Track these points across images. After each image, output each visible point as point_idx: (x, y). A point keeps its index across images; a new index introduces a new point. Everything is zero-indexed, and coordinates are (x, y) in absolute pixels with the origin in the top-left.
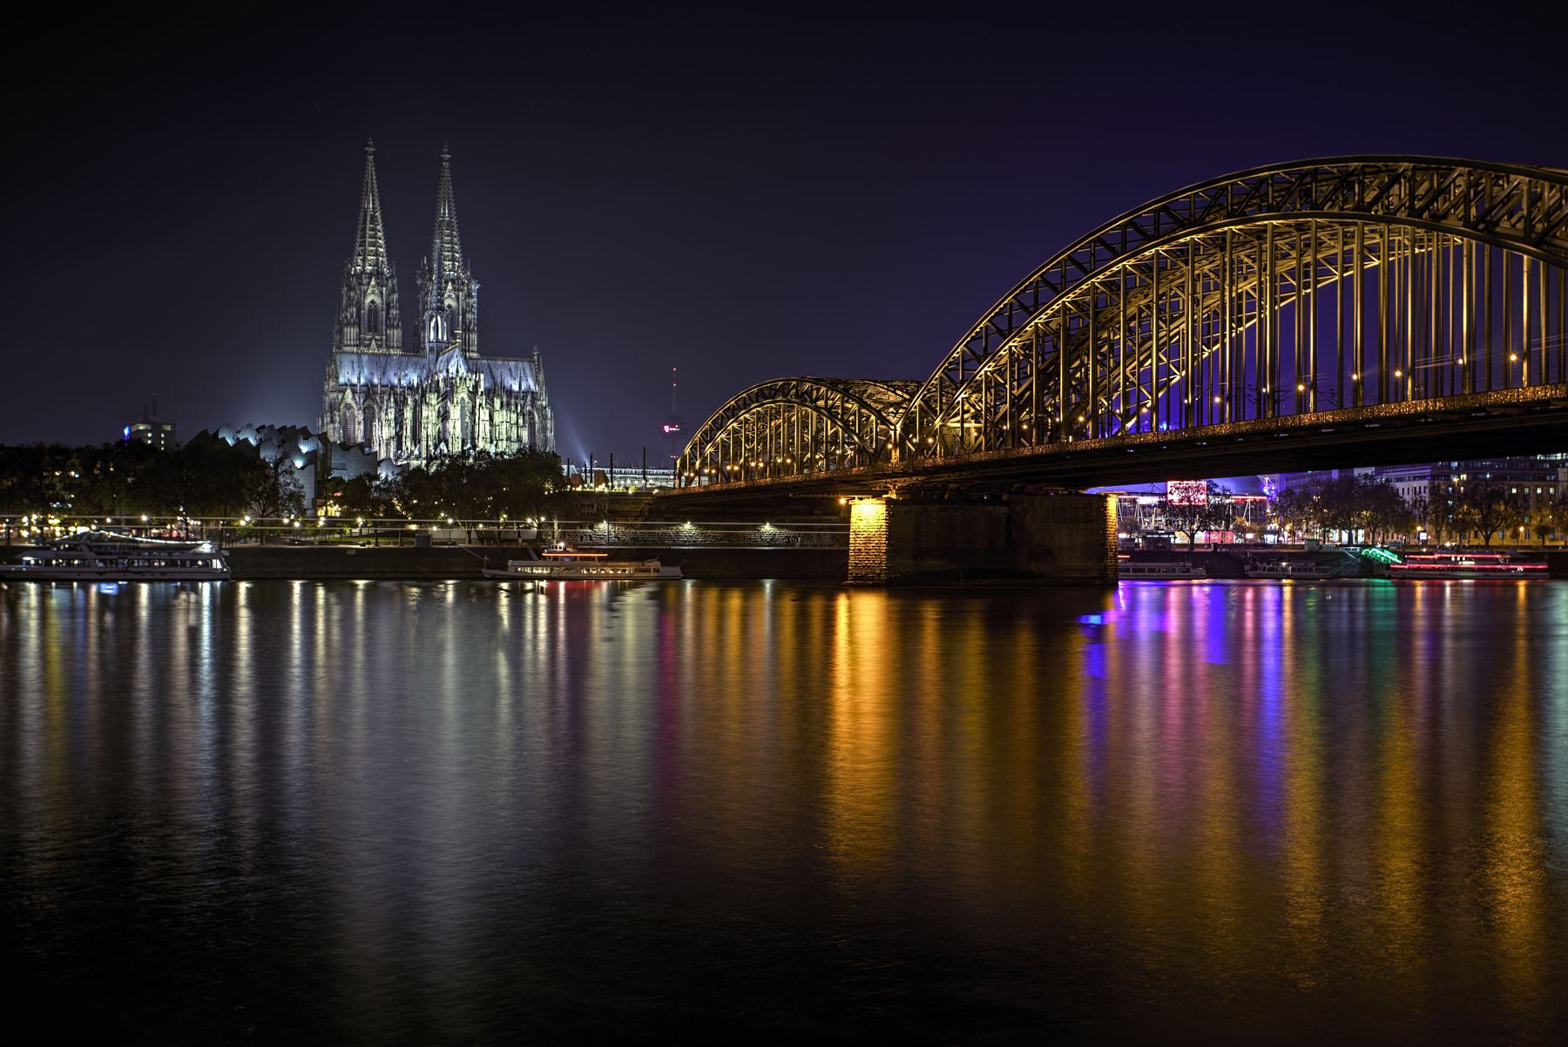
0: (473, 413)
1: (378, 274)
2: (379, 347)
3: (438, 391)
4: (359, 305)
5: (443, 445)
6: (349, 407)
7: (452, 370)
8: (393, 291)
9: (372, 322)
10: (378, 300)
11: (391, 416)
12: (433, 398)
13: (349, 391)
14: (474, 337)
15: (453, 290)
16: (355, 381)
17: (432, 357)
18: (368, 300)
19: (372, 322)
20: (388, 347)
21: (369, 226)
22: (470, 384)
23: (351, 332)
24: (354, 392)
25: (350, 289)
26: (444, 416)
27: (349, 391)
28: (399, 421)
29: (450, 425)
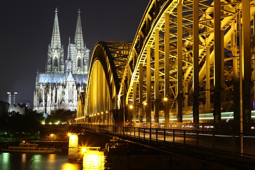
0: (73, 92)
1: (57, 48)
2: (58, 70)
4: (51, 59)
5: (63, 102)
6: (41, 90)
7: (68, 79)
10: (57, 57)
11: (50, 93)
12: (61, 87)
13: (41, 85)
16: (43, 82)
20: (60, 70)
21: (55, 34)
23: (49, 66)
24: (43, 85)
25: (49, 53)
26: (64, 93)
27: (41, 85)
28: (52, 95)
29: (65, 95)
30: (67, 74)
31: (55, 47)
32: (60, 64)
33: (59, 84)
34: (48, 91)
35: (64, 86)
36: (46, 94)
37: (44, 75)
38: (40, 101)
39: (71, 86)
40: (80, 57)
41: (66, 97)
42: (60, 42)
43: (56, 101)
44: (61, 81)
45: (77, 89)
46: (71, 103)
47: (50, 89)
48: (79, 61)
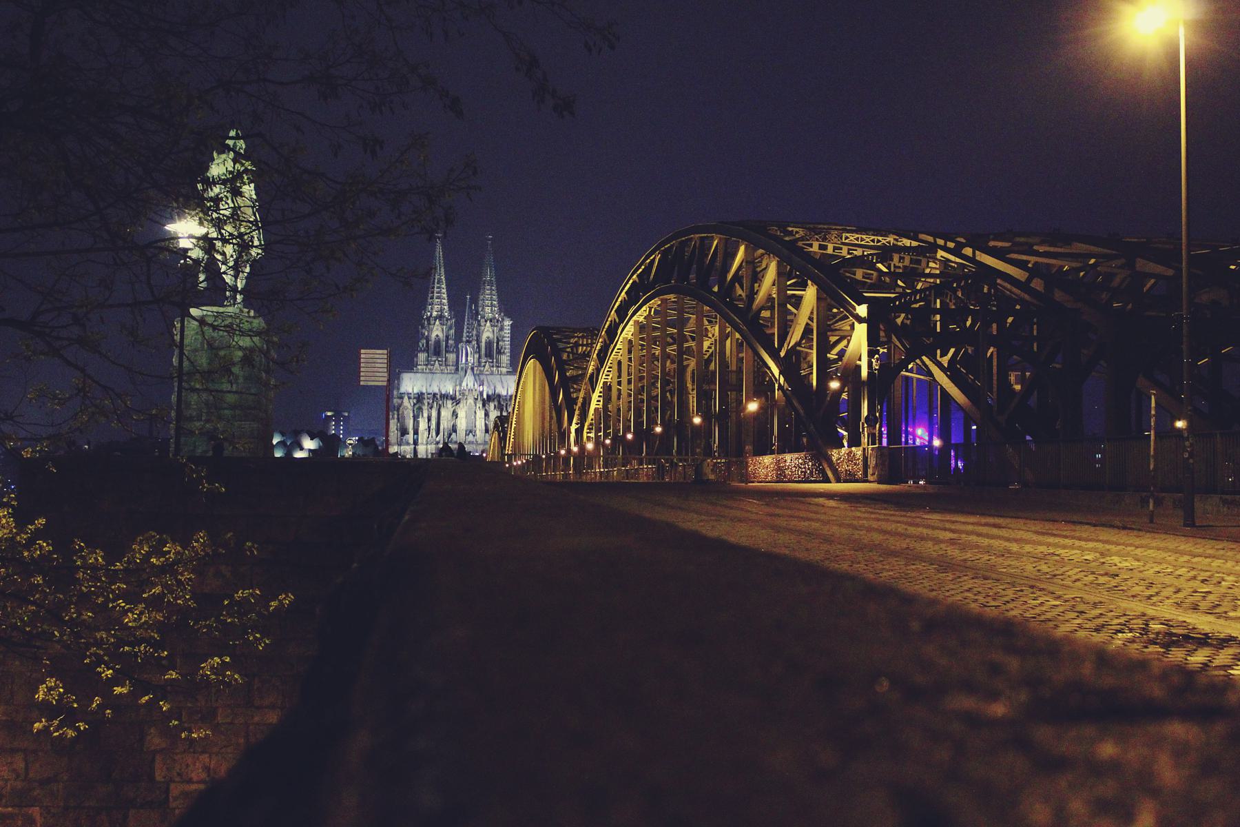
1: (440, 317)
3: (453, 398)
4: (428, 339)
7: (464, 384)
8: (450, 328)
9: (437, 350)
10: (441, 335)
11: (426, 415)
12: (449, 402)
14: (505, 359)
15: (493, 325)
17: (462, 373)
18: (434, 335)
19: (437, 350)
22: (475, 394)
23: (422, 356)
25: (423, 327)
26: (455, 414)
28: (429, 420)
29: (458, 421)
30: (461, 373)
31: (435, 314)
32: (447, 352)
33: (445, 397)
34: (420, 409)
35: (455, 400)
36: (415, 418)
37: (411, 375)
38: (404, 432)
39: (471, 401)
40: (491, 335)
41: (462, 424)
42: (445, 301)
43: (438, 433)
44: (449, 388)
45: (484, 405)
46: (470, 438)
47: (425, 408)
48: (489, 344)
